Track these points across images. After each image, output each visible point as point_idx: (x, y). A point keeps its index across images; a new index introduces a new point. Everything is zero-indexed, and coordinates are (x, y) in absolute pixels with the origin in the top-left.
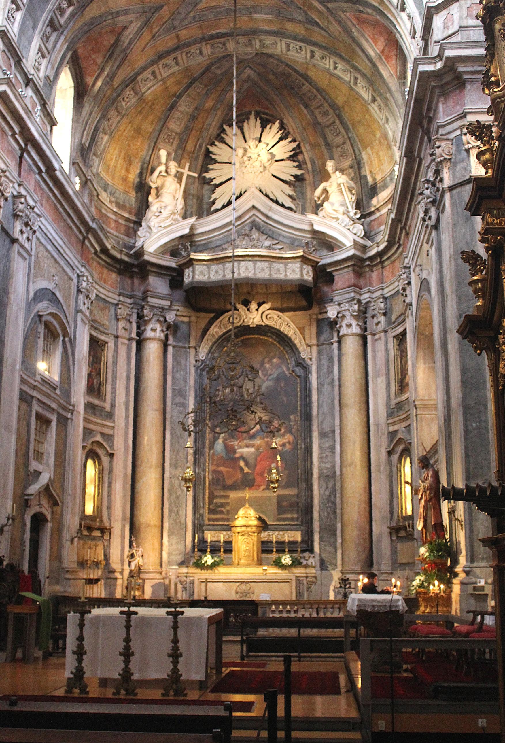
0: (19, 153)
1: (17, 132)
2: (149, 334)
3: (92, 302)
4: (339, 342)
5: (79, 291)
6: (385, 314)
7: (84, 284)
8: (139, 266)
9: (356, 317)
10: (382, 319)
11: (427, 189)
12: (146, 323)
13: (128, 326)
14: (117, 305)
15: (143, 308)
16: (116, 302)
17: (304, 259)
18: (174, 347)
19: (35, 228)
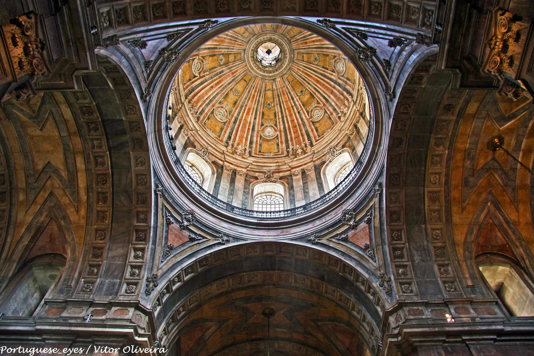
0: (464, 345)
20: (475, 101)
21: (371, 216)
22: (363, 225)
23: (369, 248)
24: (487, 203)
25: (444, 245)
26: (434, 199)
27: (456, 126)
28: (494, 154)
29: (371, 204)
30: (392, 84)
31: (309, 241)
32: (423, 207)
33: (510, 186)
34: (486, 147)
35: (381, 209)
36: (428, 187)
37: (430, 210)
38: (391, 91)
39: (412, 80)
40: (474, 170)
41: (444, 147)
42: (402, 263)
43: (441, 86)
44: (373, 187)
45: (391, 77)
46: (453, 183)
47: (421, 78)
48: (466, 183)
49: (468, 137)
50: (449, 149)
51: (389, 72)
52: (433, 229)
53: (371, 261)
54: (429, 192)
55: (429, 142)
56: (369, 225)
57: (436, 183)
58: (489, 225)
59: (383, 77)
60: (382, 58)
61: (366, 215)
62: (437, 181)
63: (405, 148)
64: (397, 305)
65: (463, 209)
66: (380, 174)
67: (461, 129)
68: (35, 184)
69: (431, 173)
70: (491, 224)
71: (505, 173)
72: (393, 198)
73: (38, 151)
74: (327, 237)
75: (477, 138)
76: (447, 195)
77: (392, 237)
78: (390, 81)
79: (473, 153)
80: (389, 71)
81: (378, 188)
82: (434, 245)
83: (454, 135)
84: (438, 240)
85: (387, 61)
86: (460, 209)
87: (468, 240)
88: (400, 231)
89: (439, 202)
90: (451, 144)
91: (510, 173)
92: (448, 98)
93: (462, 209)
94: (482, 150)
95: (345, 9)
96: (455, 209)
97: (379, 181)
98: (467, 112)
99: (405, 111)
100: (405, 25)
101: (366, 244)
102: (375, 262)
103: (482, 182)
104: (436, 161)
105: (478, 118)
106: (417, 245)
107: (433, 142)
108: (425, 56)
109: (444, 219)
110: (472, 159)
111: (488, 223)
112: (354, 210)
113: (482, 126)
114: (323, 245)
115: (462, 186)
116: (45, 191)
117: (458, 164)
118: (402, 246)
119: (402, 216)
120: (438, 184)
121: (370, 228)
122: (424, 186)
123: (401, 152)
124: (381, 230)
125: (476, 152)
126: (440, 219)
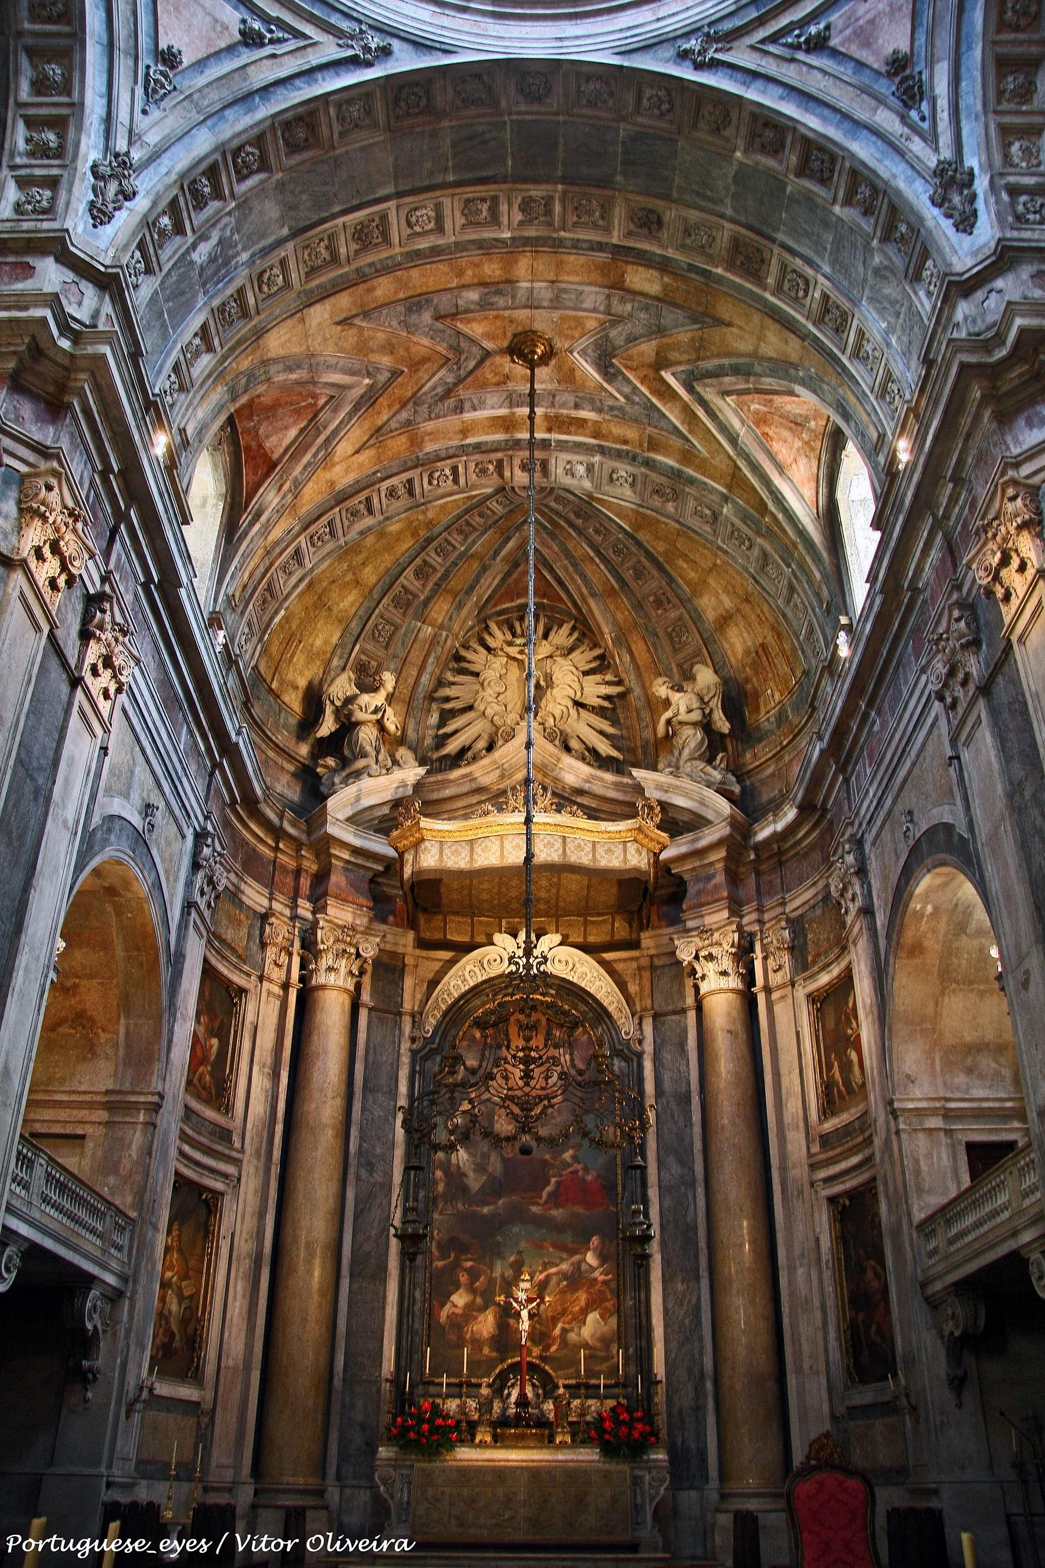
0: (112, 523)
1: (116, 469)
2: (321, 978)
3: (217, 897)
4: (699, 1008)
5: (196, 866)
6: (791, 949)
7: (206, 851)
10: (786, 958)
11: (958, 620)
12: (317, 954)
13: (284, 959)
14: (264, 917)
16: (263, 911)
18: (370, 1009)
19: (123, 679)
20: (665, 287)
21: (272, 41)
23: (172, 68)
24: (369, 375)
25: (253, 312)
26: (361, 235)
27: (584, 246)
28: (502, 352)
30: (741, 56)
32: (337, 209)
33: (415, 412)
34: (520, 329)
35: (310, 73)
36: (398, 207)
37: (332, 237)
38: (716, 51)
39: (766, 125)
40: (453, 316)
41: (521, 223)
42: (185, 214)
43: (728, 201)
44: (371, 27)
45: (767, 53)
46: (415, 273)
47: (776, 149)
48: (415, 303)
49: (553, 282)
50: (513, 239)
51: (785, 45)
52: (283, 263)
53: (139, 91)
54: (384, 217)
55: (536, 181)
56: (239, 43)
57: (409, 224)
58: (310, 401)
59: (761, 21)
60: (835, 17)
61: (267, 19)
62: (417, 229)
63: (518, 113)
64: (102, 269)
65: (345, 322)
67: (573, 260)
69: (438, 208)
70: (315, 404)
71: (448, 393)
72: (355, 111)
75: (545, 304)
76: (378, 266)
77: (240, 148)
78: (753, 48)
79: (501, 302)
80: (791, 46)
81: (373, 46)
82: (248, 286)
83: (557, 244)
84: (260, 288)
85: (826, 39)
86: (344, 316)
87: (273, 369)
88: (264, 166)
89: (356, 252)
90: (527, 241)
91: (451, 402)
92: (685, 219)
93: (346, 319)
94: (511, 322)
96: (344, 301)
97: (396, 44)
98: (630, 268)
99: (645, 103)
100: (992, 127)
101: (180, 52)
102: (144, 112)
103: (423, 343)
104: (478, 212)
105: (608, 297)
106: (232, 234)
107: (537, 192)
108: (886, 183)
109: (314, 283)
110: (484, 305)
111: (315, 397)
113: (584, 310)
115: (406, 299)
117: (470, 272)
118: (227, 192)
119: (305, 155)
120: (409, 231)
121: (230, 49)
122: (399, 195)
123: (503, 103)
124: (245, 99)
125: (506, 309)
126: (312, 272)
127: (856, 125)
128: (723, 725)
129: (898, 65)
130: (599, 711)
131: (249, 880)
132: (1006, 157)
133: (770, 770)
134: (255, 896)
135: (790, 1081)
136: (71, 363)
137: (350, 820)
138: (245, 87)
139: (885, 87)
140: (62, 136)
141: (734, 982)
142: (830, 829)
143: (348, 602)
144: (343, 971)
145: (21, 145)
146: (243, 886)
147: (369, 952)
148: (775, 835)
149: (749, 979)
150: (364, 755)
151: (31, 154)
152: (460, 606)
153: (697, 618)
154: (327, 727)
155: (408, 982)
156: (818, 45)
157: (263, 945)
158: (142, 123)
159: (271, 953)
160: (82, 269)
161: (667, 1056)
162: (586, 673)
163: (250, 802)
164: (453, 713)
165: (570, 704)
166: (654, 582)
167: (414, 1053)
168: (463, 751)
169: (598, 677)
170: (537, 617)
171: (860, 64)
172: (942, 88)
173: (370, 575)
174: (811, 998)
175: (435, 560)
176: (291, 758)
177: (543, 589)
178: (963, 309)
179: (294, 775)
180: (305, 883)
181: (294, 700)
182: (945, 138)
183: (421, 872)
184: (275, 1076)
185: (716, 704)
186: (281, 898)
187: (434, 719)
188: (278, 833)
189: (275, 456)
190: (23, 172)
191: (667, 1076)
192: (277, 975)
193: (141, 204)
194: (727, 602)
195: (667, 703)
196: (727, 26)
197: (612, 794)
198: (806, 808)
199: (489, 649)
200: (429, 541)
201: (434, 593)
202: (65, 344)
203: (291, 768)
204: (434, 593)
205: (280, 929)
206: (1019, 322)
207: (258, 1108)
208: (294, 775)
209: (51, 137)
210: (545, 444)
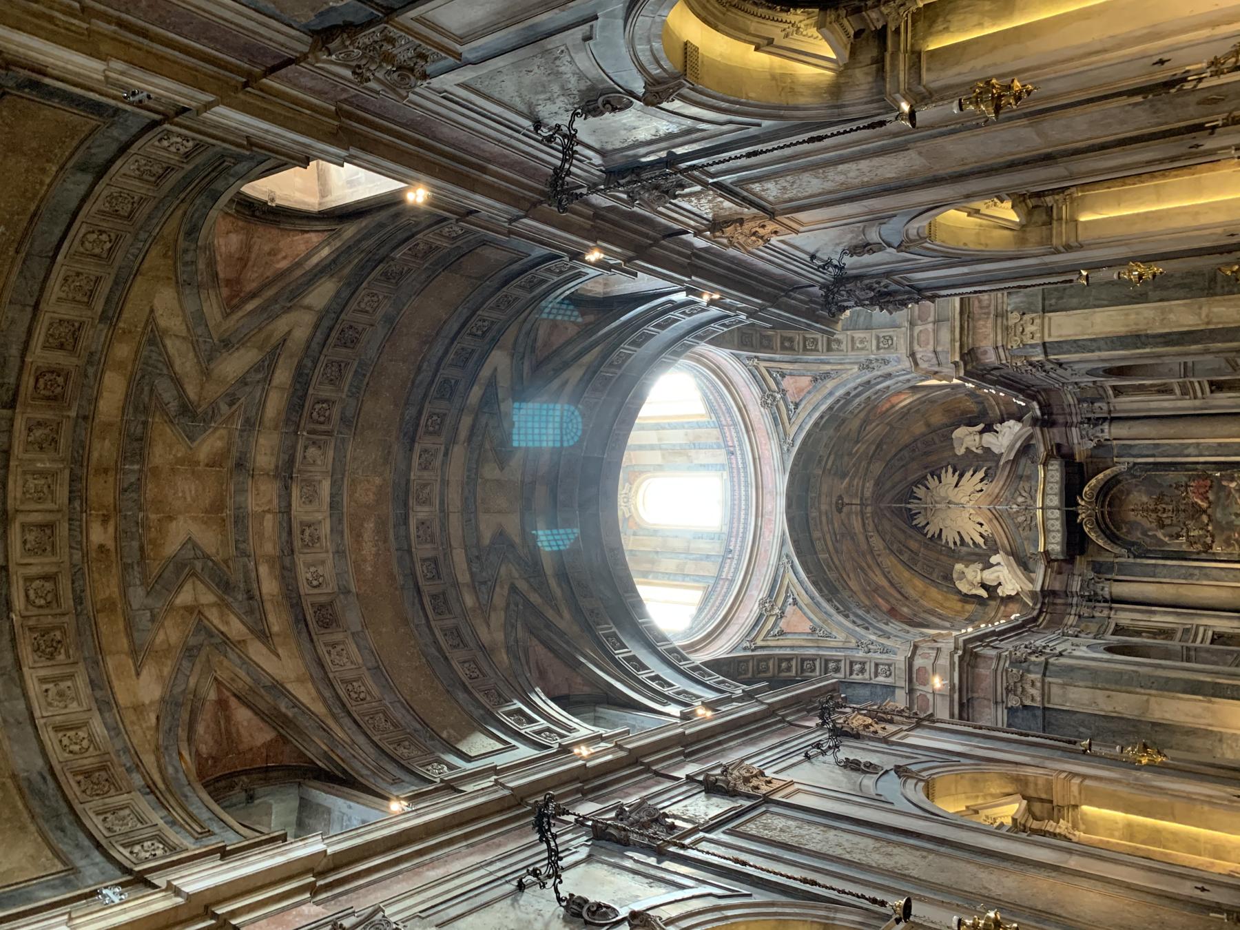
5: (1077, 636)
6: (1092, 403)
8: (1044, 597)
9: (1095, 425)
10: (1097, 405)
14: (1080, 616)
15: (1082, 596)
17: (1045, 464)
22: (789, 609)
26: (828, 566)
29: (786, 583)
31: (745, 649)
59: (783, 424)
60: (789, 398)
61: (787, 597)
66: (783, 543)
68: (484, 574)
73: (487, 511)
74: (761, 637)
95: (779, 345)
96: (845, 576)
112: (770, 595)
114: (762, 647)
116: (502, 587)
121: (801, 608)
122: (816, 553)
124: (818, 604)
127: (831, 394)
128: (981, 426)
129: (816, 379)
130: (961, 476)
131: (1065, 622)
132: (862, 349)
133: (1002, 408)
134: (1072, 620)
135: (1153, 405)
136: (965, 651)
137: (1032, 581)
138: (814, 606)
139: (819, 384)
140: (856, 663)
141: (1106, 426)
142: (1045, 390)
143: (919, 583)
144: (1101, 585)
145: (860, 676)
146: (1069, 623)
147: (1091, 575)
148: (1040, 409)
149: (1105, 419)
150: (998, 577)
151: (863, 673)
152: (911, 536)
153: (924, 435)
154: (984, 594)
155: (1101, 559)
156: (797, 405)
157: (1093, 617)
158: (841, 636)
159: (1097, 614)
160: (914, 653)
161: (1135, 452)
162: (940, 482)
163: (1035, 619)
164: (962, 539)
165: (957, 489)
166: (906, 453)
167: (1135, 557)
168: (981, 535)
169: (943, 476)
170: (909, 503)
171: (809, 392)
172: (828, 367)
173: (906, 574)
174: (1116, 396)
175: (895, 547)
176: (999, 607)
177: (900, 501)
178: (923, 365)
179: (1005, 606)
180: (1059, 601)
181: (970, 607)
182: (848, 367)
183: (1062, 552)
184: (1154, 612)
185: (971, 429)
186: (1068, 611)
187: (964, 549)
188: (1041, 612)
189: (889, 607)
190: (873, 676)
191: (1145, 452)
192: (1106, 613)
193: (873, 638)
194: (922, 422)
195: (967, 448)
196: (782, 435)
197: (1006, 473)
198: (1034, 398)
199: (928, 523)
200: (890, 549)
201: (907, 548)
202: (960, 652)
203: (1002, 608)
204: (907, 548)
205: (1086, 612)
206: (957, 359)
207: (1170, 619)
208: (1005, 606)
209: (857, 667)
210: (861, 499)
